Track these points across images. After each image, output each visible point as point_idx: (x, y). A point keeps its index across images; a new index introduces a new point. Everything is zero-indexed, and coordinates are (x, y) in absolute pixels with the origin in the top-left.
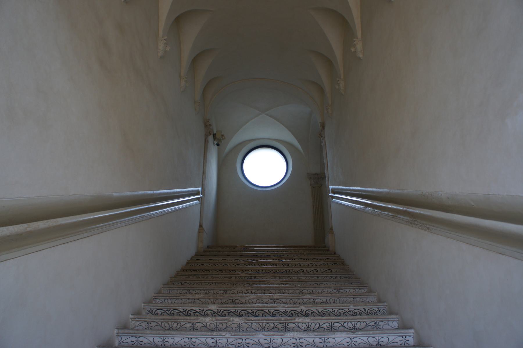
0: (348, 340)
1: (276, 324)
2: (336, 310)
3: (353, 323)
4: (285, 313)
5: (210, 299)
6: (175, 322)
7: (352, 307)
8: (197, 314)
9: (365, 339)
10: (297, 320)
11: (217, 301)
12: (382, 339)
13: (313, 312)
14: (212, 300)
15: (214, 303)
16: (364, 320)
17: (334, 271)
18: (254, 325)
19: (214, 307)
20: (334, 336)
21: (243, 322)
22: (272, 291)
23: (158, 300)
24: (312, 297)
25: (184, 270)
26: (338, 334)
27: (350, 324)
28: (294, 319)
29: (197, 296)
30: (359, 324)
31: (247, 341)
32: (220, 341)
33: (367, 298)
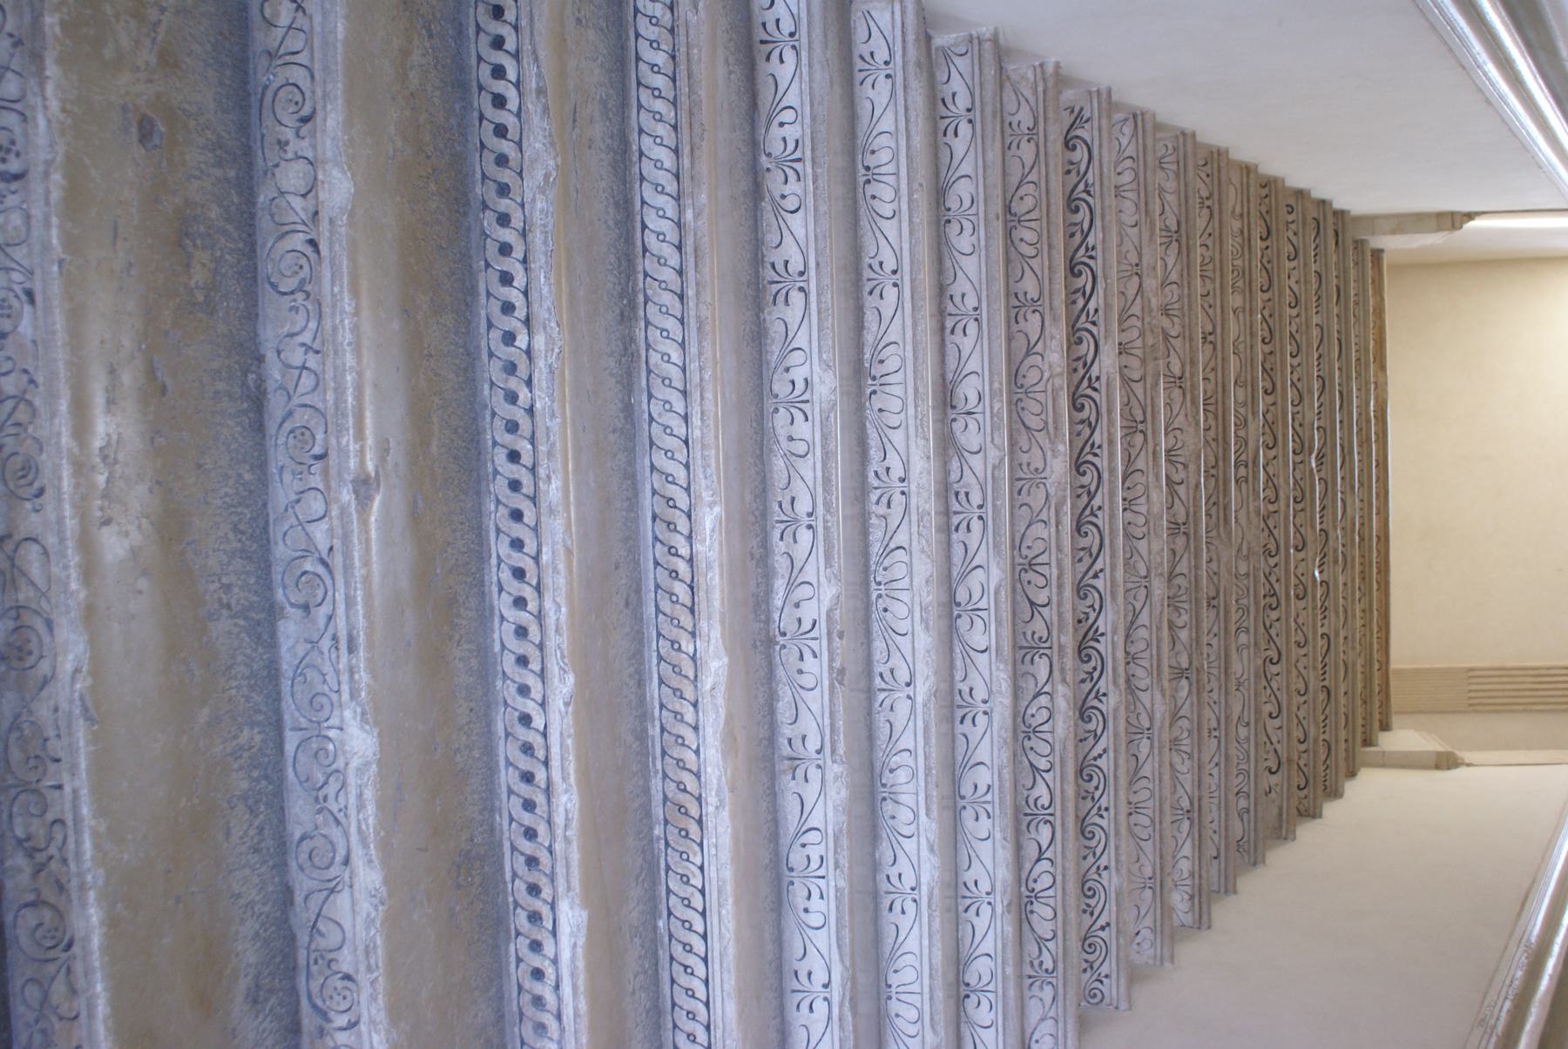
0: (985, 886)
1: (1045, 611)
2: (1104, 823)
3: (1051, 892)
5: (1142, 334)
6: (1040, 236)
7: (1115, 879)
8: (1081, 302)
9: (988, 946)
10: (1061, 688)
11: (1135, 363)
12: (985, 1005)
13: (1097, 738)
14: (1139, 343)
15: (1123, 349)
16: (1060, 933)
17: (1274, 779)
18: (1039, 530)
19: (1107, 363)
20: (998, 835)
21: (1052, 491)
22: (1184, 563)
24: (1157, 724)
25: (1270, 185)
27: (1046, 880)
28: (1064, 681)
29: (1151, 284)
31: (976, 525)
32: (973, 426)
33: (1154, 931)
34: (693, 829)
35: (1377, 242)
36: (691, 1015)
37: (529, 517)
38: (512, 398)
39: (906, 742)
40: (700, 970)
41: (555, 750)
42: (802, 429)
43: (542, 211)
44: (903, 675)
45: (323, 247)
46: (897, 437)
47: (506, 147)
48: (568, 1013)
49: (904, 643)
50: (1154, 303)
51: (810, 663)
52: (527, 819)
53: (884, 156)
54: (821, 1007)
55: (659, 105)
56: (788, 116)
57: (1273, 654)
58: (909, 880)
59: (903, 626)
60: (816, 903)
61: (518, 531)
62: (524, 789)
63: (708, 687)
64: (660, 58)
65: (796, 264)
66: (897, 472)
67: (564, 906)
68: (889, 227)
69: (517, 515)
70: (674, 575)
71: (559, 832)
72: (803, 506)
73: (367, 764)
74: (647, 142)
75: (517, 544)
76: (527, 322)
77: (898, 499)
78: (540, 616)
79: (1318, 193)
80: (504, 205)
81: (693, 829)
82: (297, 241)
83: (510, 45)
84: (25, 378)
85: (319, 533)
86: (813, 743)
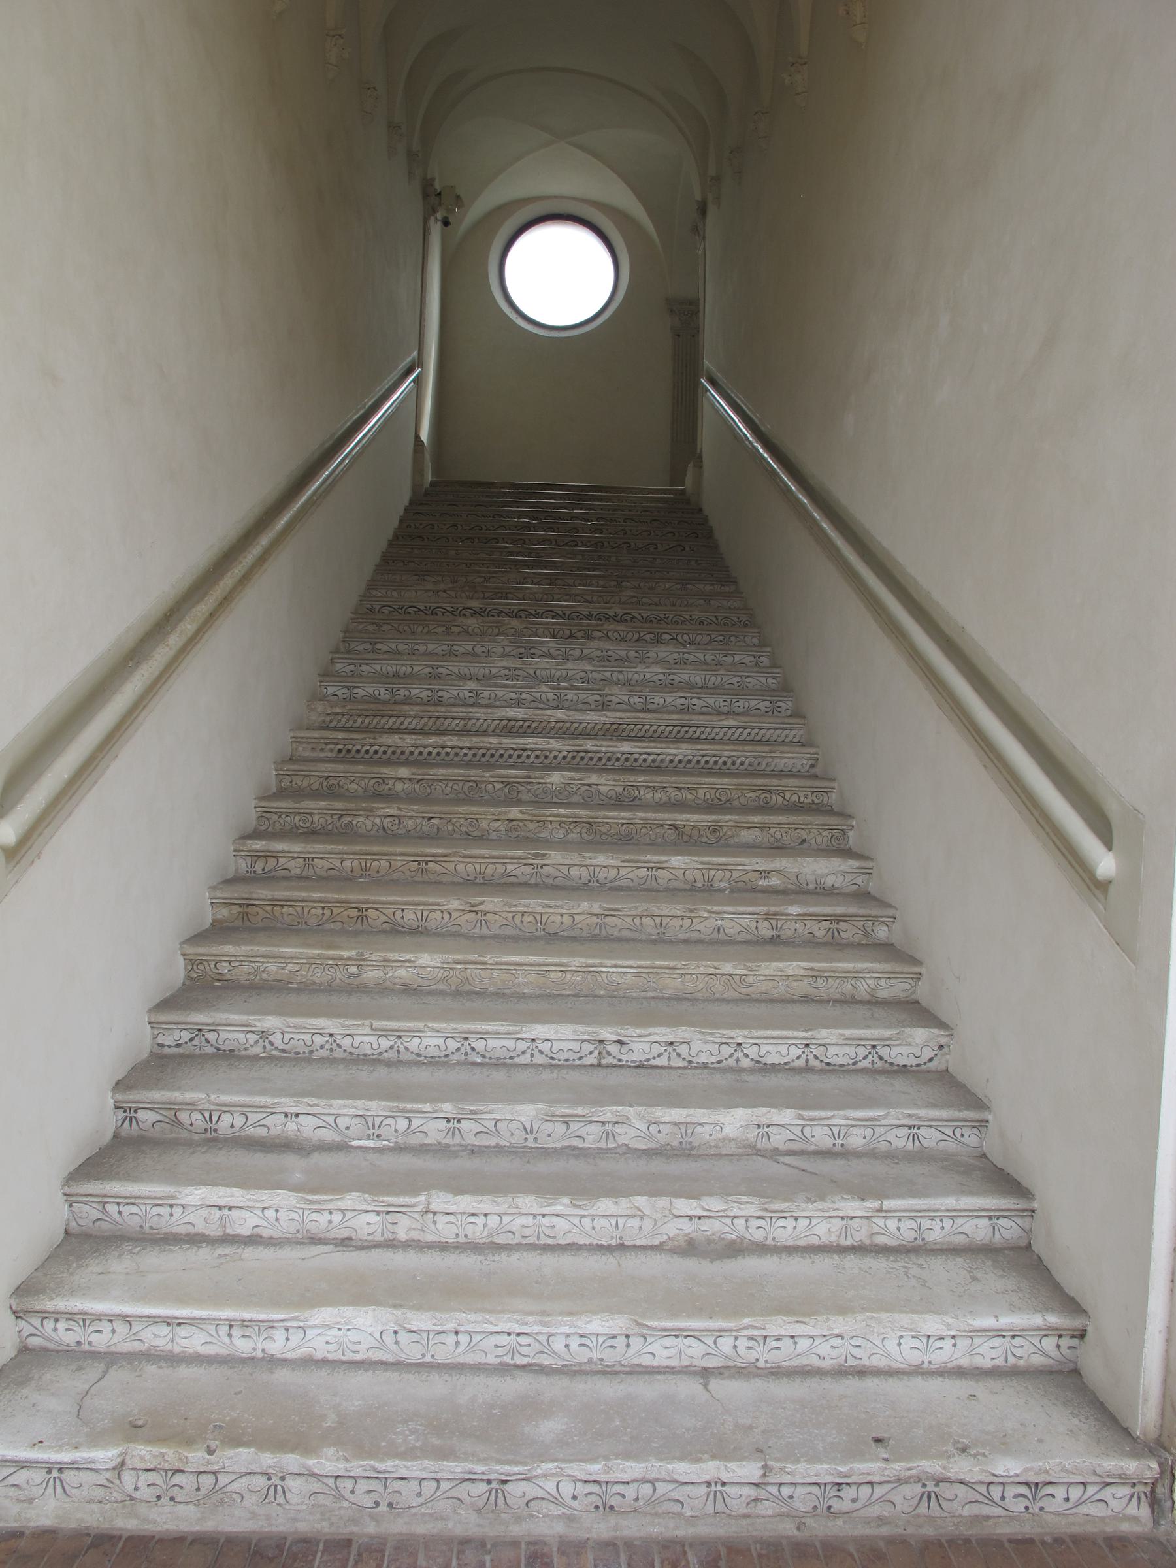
0: (676, 656)
4: (589, 617)
7: (696, 613)
9: (701, 656)
10: (606, 627)
17: (687, 549)
18: (540, 631)
23: (374, 592)
25: (396, 537)
26: (663, 647)
27: (686, 637)
29: (442, 586)
30: (699, 637)
31: (532, 651)
34: (615, 726)
35: (427, 484)
36: (679, 732)
37: (502, 752)
38: (466, 755)
39: (608, 674)
40: (663, 728)
42: (486, 694)
44: (583, 674)
46: (494, 671)
47: (390, 751)
48: (659, 751)
49: (571, 673)
50: (451, 585)
51: (569, 697)
52: (595, 760)
53: (389, 669)
54: (694, 701)
55: (375, 721)
56: (377, 692)
57: (625, 546)
58: (661, 677)
59: (564, 673)
60: (656, 700)
61: (506, 756)
62: (586, 760)
64: (360, 720)
65: (429, 693)
66: (507, 672)
67: (622, 749)
68: (416, 669)
69: (502, 756)
70: (529, 727)
72: (513, 695)
74: (386, 726)
75: (510, 756)
76: (443, 748)
77: (517, 672)
78: (533, 750)
79: (401, 512)
80: (407, 753)
81: (615, 726)
82: (417, 786)
83: (359, 747)
85: (498, 786)
86: (597, 698)
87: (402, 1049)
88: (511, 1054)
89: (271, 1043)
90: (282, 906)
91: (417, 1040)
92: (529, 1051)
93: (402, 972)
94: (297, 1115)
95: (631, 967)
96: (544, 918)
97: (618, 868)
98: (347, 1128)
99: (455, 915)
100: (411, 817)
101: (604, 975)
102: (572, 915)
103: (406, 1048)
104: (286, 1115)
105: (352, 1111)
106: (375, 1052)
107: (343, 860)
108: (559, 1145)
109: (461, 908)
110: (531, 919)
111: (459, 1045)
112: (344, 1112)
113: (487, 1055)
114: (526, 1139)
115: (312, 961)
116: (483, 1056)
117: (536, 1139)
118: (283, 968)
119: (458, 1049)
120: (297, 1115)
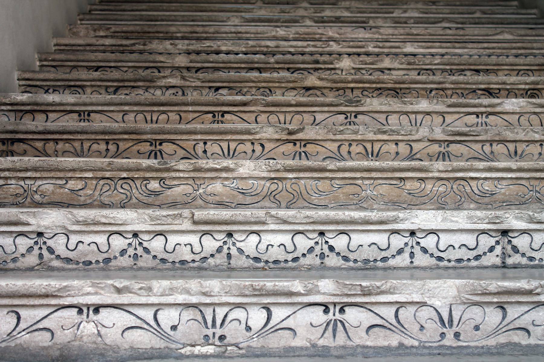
41: (354, 50)
43: (182, 46)
45: (199, 65)
63: (338, 36)
71: (381, 50)
73: (352, 60)
84: (239, 94)
87: (234, 251)
88: (384, 254)
89: (51, 250)
90: (56, 141)
91: (254, 238)
92: (408, 250)
93: (217, 187)
94: (97, 309)
95: (509, 170)
96: (377, 146)
97: (442, 114)
98: (174, 328)
99: (269, 146)
100: (196, 88)
101: (473, 183)
102: (409, 143)
103: (240, 251)
104: (80, 311)
105: (181, 298)
106: (197, 258)
107: (126, 113)
108: (492, 342)
109: (276, 136)
110: (360, 149)
111: (311, 243)
112: (170, 299)
113: (352, 256)
114: (443, 335)
115: (100, 174)
116: (346, 259)
117: (457, 335)
118: (61, 187)
119: (311, 250)
120: (97, 309)
